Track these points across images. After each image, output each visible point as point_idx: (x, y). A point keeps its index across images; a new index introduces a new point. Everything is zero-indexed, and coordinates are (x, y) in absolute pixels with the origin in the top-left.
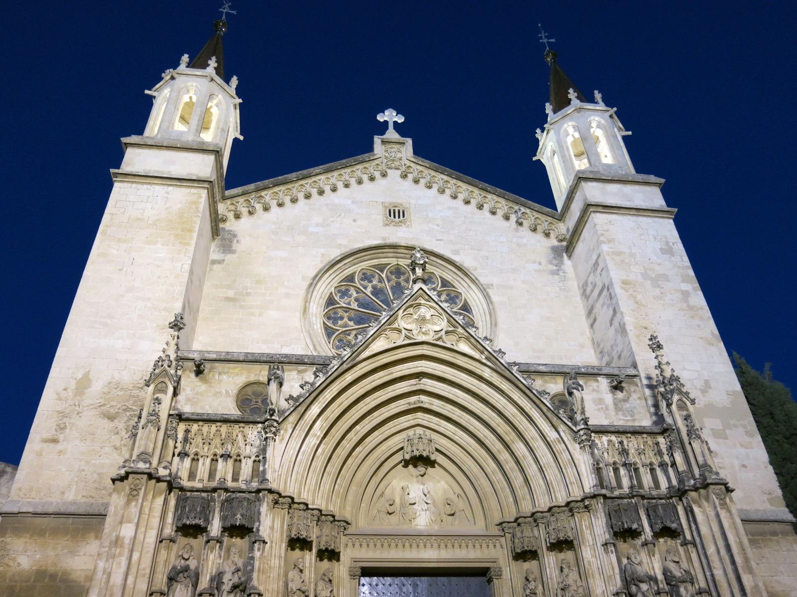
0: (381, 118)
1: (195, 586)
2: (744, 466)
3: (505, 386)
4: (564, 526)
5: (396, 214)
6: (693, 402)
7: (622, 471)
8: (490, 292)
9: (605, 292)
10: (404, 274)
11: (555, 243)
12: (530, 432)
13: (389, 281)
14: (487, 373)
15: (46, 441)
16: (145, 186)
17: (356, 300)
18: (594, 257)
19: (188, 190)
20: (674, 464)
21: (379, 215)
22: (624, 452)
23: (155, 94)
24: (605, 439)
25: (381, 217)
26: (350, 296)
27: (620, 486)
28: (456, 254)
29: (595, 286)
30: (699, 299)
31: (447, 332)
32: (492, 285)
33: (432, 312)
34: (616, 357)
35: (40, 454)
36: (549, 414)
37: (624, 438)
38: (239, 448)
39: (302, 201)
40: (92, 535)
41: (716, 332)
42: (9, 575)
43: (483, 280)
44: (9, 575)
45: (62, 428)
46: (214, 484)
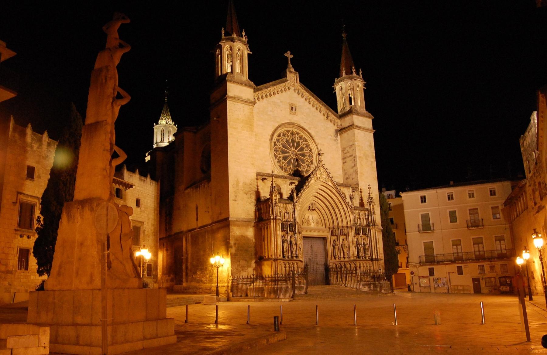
3: (337, 195)
4: (345, 231)
9: (352, 157)
14: (334, 191)
18: (351, 143)
21: (288, 110)
34: (351, 178)
39: (265, 99)
43: (317, 141)
45: (236, 196)
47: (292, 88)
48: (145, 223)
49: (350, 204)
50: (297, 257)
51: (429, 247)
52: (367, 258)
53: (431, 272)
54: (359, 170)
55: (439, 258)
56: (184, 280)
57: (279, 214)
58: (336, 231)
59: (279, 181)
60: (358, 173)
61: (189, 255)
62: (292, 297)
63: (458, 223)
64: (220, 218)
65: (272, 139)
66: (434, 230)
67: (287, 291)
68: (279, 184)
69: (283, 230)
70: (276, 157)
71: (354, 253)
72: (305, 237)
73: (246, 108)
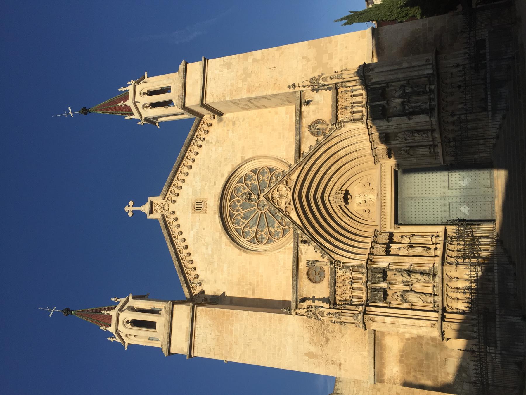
0: (130, 214)
1: (407, 291)
2: (346, 47)
5: (199, 206)
6: (323, 74)
7: (355, 109)
8: (246, 158)
10: (235, 203)
11: (215, 120)
13: (239, 211)
14: (307, 167)
15: (340, 368)
16: (196, 340)
17: (250, 227)
18: (231, 104)
19: (198, 316)
20: (352, 87)
21: (199, 216)
22: (346, 107)
23: (126, 344)
24: (339, 116)
25: (201, 215)
26: (248, 231)
27: (361, 111)
28: (224, 175)
29: (246, 105)
30: (258, 54)
31: (287, 184)
32: (242, 157)
33: (276, 191)
35: (347, 371)
36: (328, 139)
37: (339, 107)
38: (347, 278)
39: (192, 257)
40: (383, 342)
41: (276, 48)
42: (402, 375)
43: (239, 162)
44: (402, 375)
46: (364, 288)
47: (172, 207)
52: (433, 87)
60: (275, 93)
71: (421, 120)
72: (396, 222)
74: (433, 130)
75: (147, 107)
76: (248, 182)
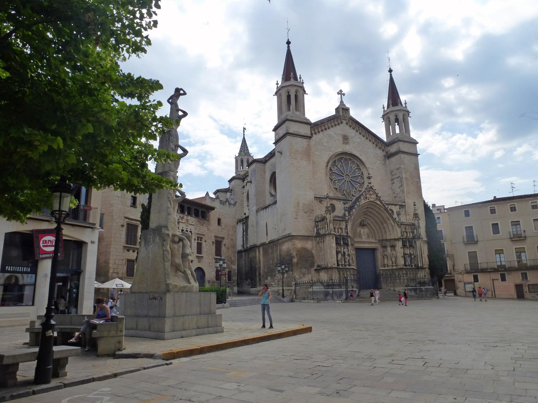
4: (393, 243)
12: (388, 222)
20: (414, 232)
39: (321, 132)
43: (367, 166)
47: (344, 122)
48: (226, 238)
49: (397, 219)
50: (349, 265)
51: (473, 256)
53: (476, 279)
54: (405, 189)
55: (484, 266)
56: (258, 284)
57: (333, 230)
58: (385, 243)
59: (334, 202)
60: (405, 192)
61: (262, 264)
62: (346, 299)
63: (501, 234)
64: (285, 234)
65: (327, 166)
66: (478, 241)
67: (341, 294)
68: (335, 204)
69: (338, 244)
70: (331, 180)
71: (401, 262)
72: (357, 249)
73: (304, 141)
74: (396, 266)
75: (396, 116)
76: (357, 170)
